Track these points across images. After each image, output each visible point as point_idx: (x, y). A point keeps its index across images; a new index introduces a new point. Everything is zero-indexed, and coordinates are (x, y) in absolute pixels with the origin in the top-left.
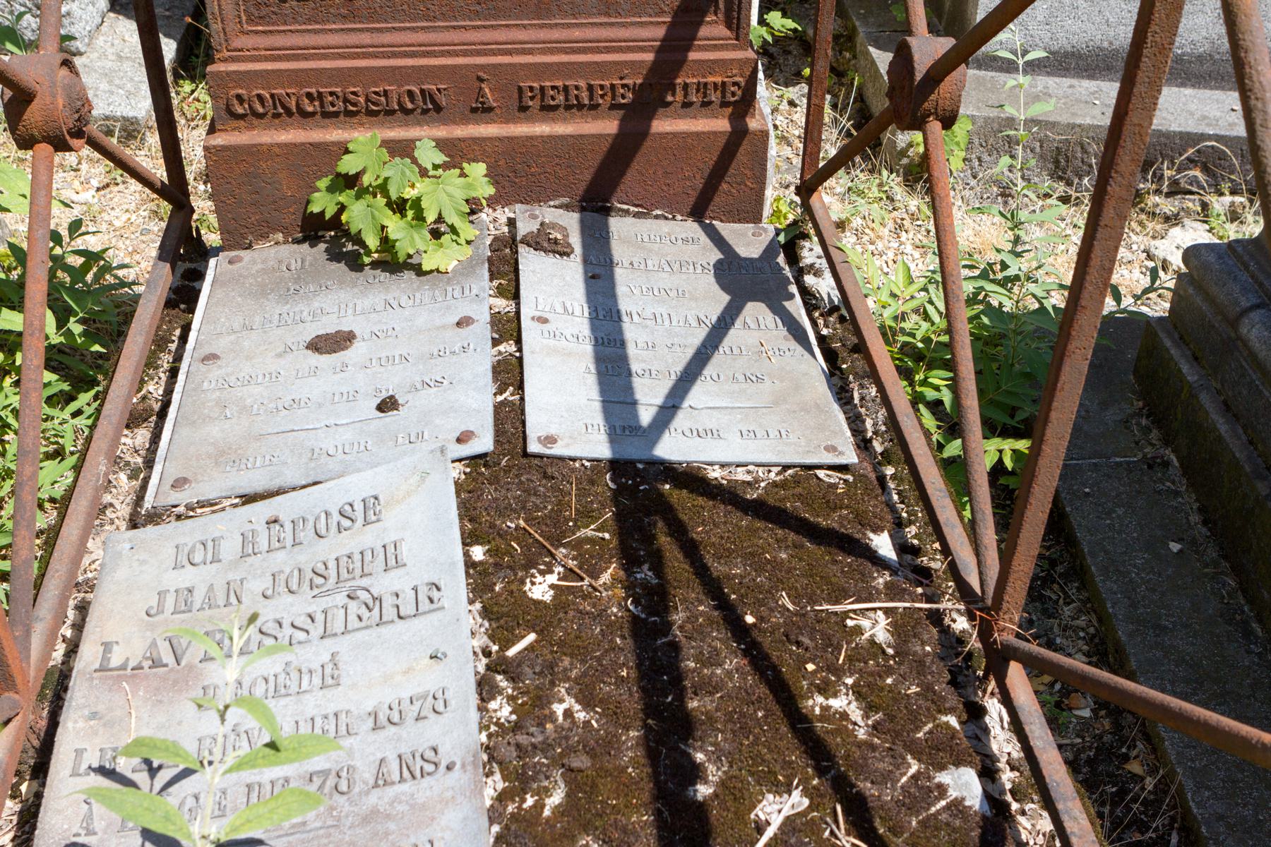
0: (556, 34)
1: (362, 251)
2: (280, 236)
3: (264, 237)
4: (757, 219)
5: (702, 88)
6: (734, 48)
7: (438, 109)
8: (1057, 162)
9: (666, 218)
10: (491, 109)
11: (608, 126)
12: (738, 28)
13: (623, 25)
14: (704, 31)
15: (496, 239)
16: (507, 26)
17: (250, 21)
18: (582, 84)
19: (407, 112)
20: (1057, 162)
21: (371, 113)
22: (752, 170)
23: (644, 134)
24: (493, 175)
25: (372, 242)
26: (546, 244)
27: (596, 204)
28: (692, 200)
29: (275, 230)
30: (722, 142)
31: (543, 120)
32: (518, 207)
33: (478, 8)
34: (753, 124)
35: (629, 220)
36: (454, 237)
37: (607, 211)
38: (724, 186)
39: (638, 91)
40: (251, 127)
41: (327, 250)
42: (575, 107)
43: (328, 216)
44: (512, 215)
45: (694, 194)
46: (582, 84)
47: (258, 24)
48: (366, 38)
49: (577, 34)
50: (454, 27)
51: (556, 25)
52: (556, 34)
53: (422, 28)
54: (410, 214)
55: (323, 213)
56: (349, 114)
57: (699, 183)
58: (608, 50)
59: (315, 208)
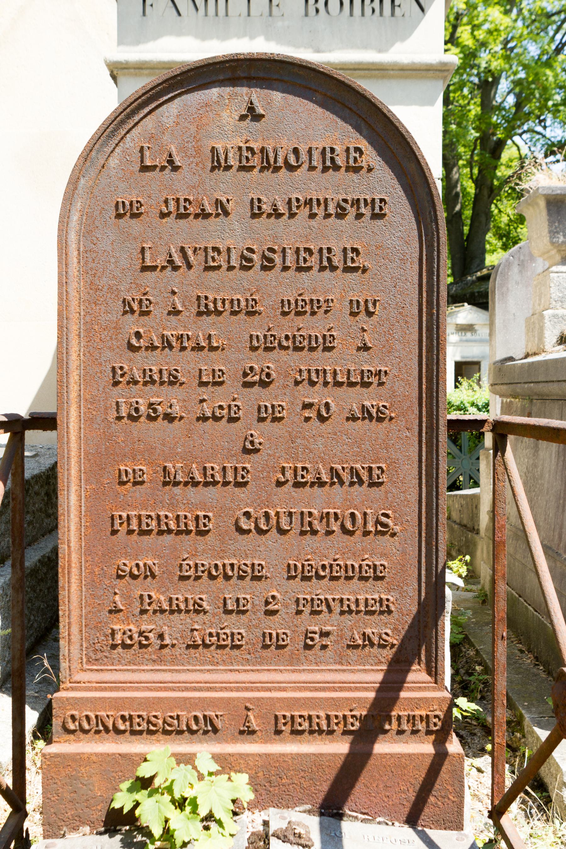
1: (148, 841)
2: (87, 829)
3: (75, 829)
4: (459, 826)
5: (411, 719)
6: (434, 689)
7: (215, 730)
9: (387, 824)
10: (253, 732)
11: (341, 747)
12: (436, 674)
13: (352, 671)
14: (411, 677)
15: (253, 834)
16: (268, 670)
17: (89, 662)
18: (322, 714)
19: (192, 732)
21: (166, 733)
22: (453, 785)
23: (369, 754)
24: (254, 784)
25: (157, 831)
26: (291, 838)
27: (332, 809)
28: (406, 810)
29: (84, 824)
30: (428, 762)
31: (293, 742)
32: (271, 810)
33: (248, 657)
35: (358, 824)
36: (221, 830)
37: (340, 816)
38: (432, 799)
39: (364, 720)
40: (78, 741)
41: (121, 840)
43: (125, 811)
44: (266, 818)
45: (409, 805)
46: (322, 714)
47: (94, 664)
48: (167, 677)
49: (318, 677)
50: (231, 670)
51: (304, 670)
53: (208, 671)
54: (188, 809)
55: (122, 808)
56: (150, 732)
57: (412, 796)
58: (341, 689)
59: (116, 805)
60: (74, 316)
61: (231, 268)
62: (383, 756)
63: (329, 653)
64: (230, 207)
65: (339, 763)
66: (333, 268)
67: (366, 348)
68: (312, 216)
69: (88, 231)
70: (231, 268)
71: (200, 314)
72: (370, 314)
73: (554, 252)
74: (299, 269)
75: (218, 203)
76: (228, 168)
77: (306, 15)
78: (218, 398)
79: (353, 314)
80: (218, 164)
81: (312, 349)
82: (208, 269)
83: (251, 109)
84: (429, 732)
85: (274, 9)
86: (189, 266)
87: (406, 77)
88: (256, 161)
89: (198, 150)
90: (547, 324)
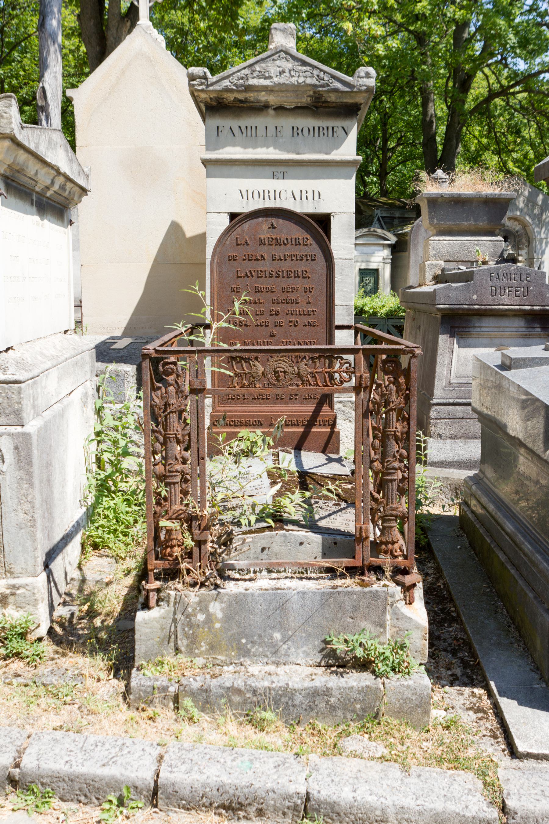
0: (289, 408)
5: (323, 421)
7: (261, 425)
8: (456, 492)
11: (302, 430)
14: (323, 408)
19: (254, 425)
20: (456, 492)
21: (246, 426)
23: (310, 431)
27: (298, 448)
30: (328, 434)
34: (336, 430)
37: (300, 450)
39: (308, 421)
42: (293, 425)
48: (246, 408)
49: (294, 408)
52: (289, 408)
56: (241, 426)
57: (323, 444)
60: (216, 293)
61: (266, 277)
62: (314, 432)
63: (297, 401)
64: (265, 257)
65: (300, 435)
66: (299, 277)
67: (309, 303)
68: (292, 260)
69: (220, 265)
70: (266, 277)
71: (256, 292)
72: (311, 292)
73: (432, 228)
74: (288, 277)
75: (262, 256)
76: (265, 244)
77: (293, 136)
78: (262, 320)
79: (305, 292)
80: (262, 243)
81: (292, 303)
82: (259, 277)
83: (272, 225)
84: (329, 425)
85: (278, 133)
86: (252, 276)
87: (339, 166)
88: (274, 242)
89: (255, 239)
90: (427, 269)
